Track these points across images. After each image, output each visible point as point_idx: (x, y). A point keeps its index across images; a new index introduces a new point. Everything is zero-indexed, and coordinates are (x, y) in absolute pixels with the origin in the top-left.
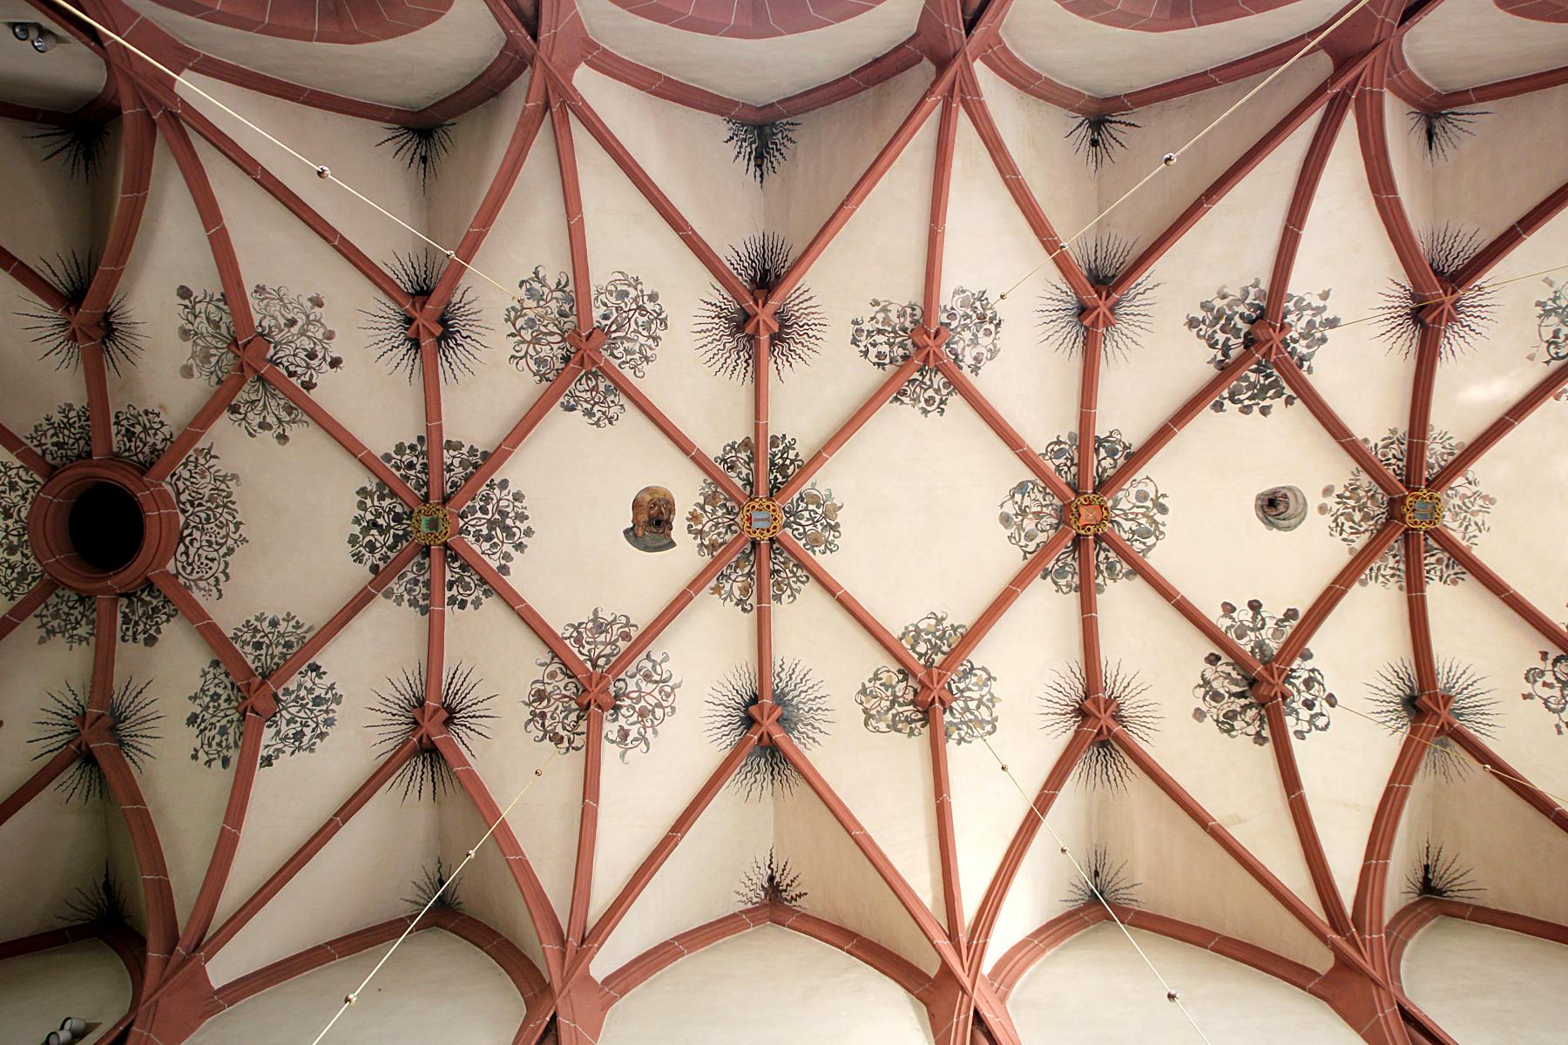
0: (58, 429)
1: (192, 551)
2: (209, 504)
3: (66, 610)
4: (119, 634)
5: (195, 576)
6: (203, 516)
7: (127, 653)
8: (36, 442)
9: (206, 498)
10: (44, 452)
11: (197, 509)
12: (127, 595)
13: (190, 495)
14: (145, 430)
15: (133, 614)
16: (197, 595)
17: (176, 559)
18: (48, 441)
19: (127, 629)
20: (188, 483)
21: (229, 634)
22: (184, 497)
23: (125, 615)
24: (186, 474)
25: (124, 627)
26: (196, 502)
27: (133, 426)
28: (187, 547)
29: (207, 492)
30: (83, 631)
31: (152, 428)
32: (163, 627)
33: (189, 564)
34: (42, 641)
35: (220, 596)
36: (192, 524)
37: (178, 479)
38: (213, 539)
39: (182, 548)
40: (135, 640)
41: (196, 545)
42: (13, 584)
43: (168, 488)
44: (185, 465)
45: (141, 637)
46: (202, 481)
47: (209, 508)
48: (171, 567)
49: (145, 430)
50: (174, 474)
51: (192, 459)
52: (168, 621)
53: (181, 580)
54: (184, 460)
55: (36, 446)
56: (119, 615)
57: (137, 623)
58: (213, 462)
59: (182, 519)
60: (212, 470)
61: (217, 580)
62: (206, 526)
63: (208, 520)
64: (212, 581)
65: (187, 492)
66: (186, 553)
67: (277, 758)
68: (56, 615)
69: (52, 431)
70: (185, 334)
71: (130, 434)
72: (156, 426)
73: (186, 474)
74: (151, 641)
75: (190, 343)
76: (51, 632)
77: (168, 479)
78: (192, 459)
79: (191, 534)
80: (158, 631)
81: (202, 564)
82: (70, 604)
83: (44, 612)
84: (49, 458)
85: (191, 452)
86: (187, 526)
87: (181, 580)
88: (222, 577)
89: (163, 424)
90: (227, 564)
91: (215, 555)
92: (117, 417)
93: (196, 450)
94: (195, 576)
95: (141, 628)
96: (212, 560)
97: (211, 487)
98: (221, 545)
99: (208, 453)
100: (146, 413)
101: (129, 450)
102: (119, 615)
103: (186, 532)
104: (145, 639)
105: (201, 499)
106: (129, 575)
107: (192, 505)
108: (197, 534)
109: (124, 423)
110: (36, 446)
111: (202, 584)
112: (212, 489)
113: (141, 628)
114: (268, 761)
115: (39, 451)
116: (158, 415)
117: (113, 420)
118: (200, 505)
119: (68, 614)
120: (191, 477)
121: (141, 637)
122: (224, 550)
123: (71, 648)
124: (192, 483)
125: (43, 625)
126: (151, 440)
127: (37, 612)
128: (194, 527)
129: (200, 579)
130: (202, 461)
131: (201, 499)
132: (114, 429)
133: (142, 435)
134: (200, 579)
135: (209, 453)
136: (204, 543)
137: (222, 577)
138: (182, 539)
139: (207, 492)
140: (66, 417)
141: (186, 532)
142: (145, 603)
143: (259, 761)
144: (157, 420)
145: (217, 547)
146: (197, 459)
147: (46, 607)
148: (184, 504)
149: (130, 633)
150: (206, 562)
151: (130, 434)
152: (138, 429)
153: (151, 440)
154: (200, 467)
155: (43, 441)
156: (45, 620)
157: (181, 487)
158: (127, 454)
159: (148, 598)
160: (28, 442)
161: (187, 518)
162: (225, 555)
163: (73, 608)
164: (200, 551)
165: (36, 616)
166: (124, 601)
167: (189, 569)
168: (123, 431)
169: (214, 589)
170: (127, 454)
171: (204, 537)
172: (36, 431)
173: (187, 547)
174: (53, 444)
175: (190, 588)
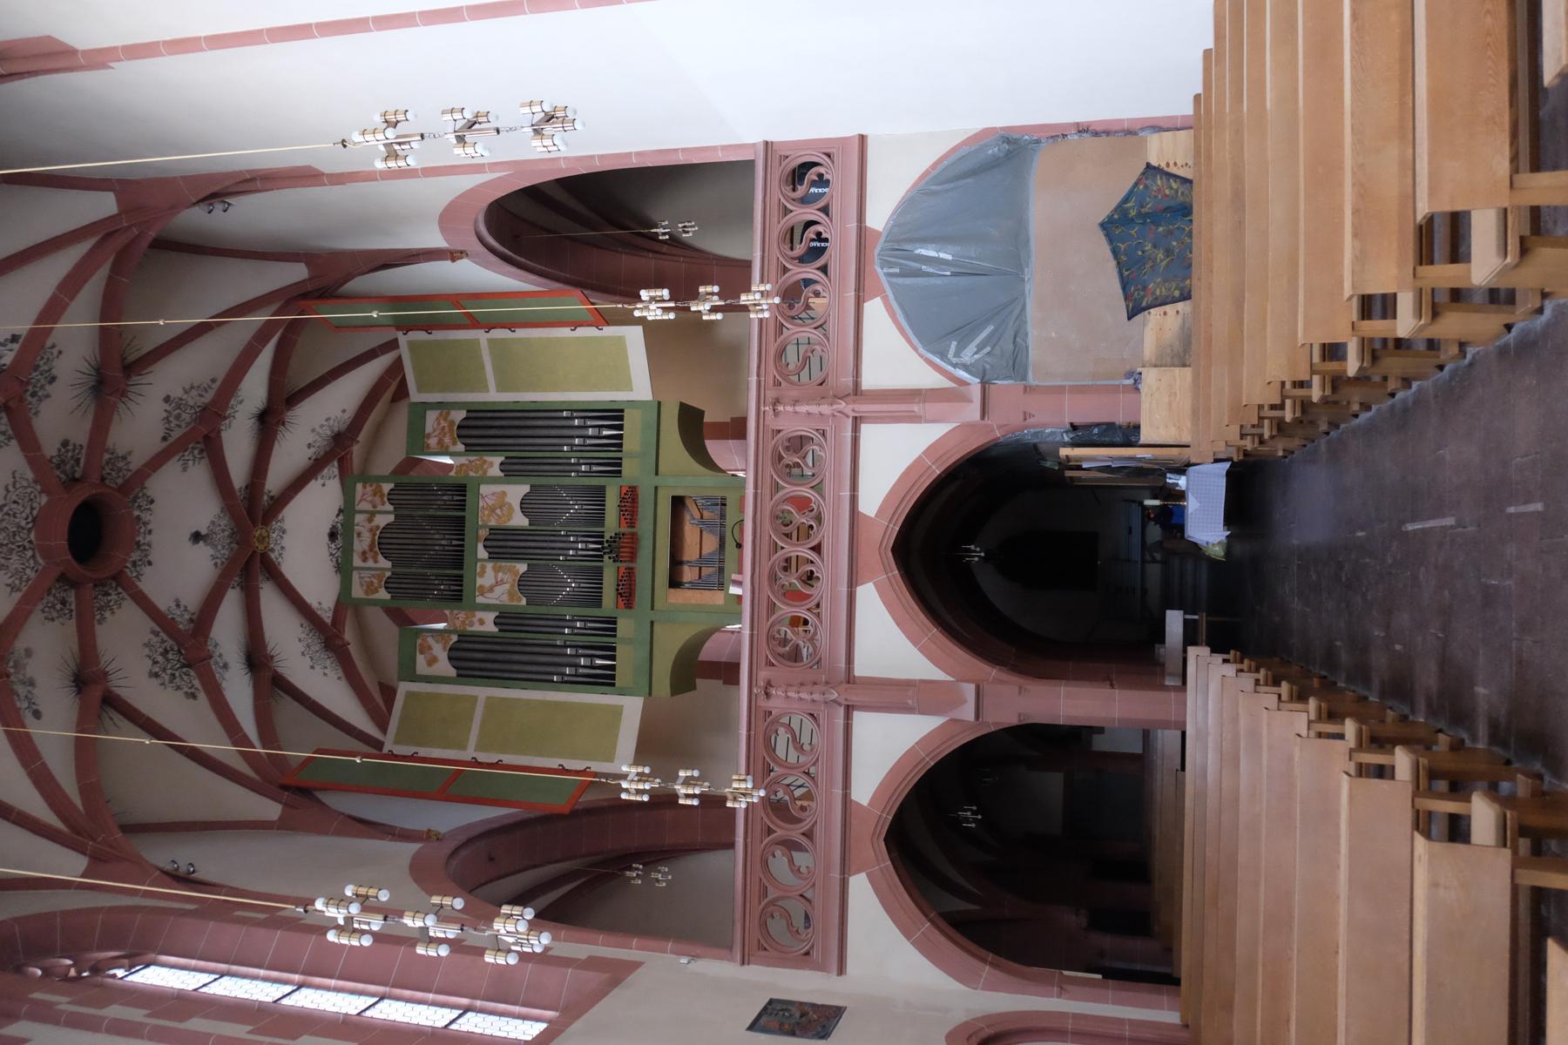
0: (107, 606)
1: (28, 510)
2: (13, 547)
3: (113, 473)
4: (84, 451)
5: (29, 490)
6: (18, 538)
7: (80, 434)
8: (121, 596)
9: (15, 551)
10: (116, 589)
11: (20, 544)
12: (76, 480)
13: (26, 555)
14: (53, 607)
15: (73, 467)
16: (30, 475)
17: (40, 504)
18: (114, 597)
19: (78, 454)
20: (27, 564)
21: (14, 442)
22: (29, 553)
23: (78, 464)
24: (28, 571)
25: (79, 456)
26: (21, 549)
27: (62, 610)
28: (31, 513)
29: (14, 557)
30: (107, 456)
31: (50, 607)
32: (55, 453)
33: (31, 500)
34: (130, 453)
35: (14, 473)
36: (25, 531)
37: (33, 567)
38: (12, 519)
39: (35, 512)
40: (75, 445)
41: (24, 515)
42: (140, 495)
43: (40, 561)
44: (28, 579)
45: (71, 447)
46: (17, 566)
47: (12, 543)
48: (44, 499)
49: (53, 607)
50: (37, 571)
51: (24, 584)
52: (52, 457)
53: (39, 488)
54: (30, 582)
55: (120, 593)
56: (82, 464)
57: (72, 457)
58: (10, 581)
59: (32, 536)
60: (10, 575)
61: (14, 487)
62: (14, 529)
63: (14, 535)
64: (18, 485)
65: (28, 557)
66: (32, 509)
67: (6, 340)
68: (120, 470)
69: (111, 604)
70: (32, 683)
71: (64, 603)
72: (47, 609)
73: (28, 571)
74: (65, 444)
75: (28, 676)
76: (124, 458)
77: (40, 568)
78: (24, 584)
79: (28, 523)
80: (59, 450)
81: (23, 500)
82: (110, 477)
83: (125, 472)
84: (114, 585)
85: (25, 589)
86: (29, 530)
87: (39, 488)
88: (11, 488)
89: (43, 611)
90: (5, 498)
91: (14, 506)
92: (71, 616)
93: (21, 591)
94: (29, 490)
95: (70, 454)
96: (15, 502)
97: (11, 561)
98: (7, 514)
99: (13, 588)
100: (53, 620)
101: (65, 590)
102: (82, 464)
103: (30, 525)
104: (68, 445)
105: (18, 552)
106: (81, 494)
107: (24, 547)
108: (23, 523)
109: (67, 611)
110: (120, 593)
111: (25, 484)
112: (10, 559)
113: (70, 454)
114: (14, 339)
115: (120, 590)
116: (46, 618)
117: (74, 613)
118: (19, 547)
119: (112, 470)
120: (24, 569)
121: (71, 447)
122: (6, 509)
123: (114, 445)
124: (23, 564)
125: (128, 463)
126: (51, 598)
127: (130, 474)
128: (23, 529)
129: (26, 488)
130: (17, 582)
131: (18, 552)
132: (73, 607)
133: (56, 602)
134: (26, 488)
135: (12, 588)
136: (18, 515)
137: (11, 488)
138: (34, 520)
139: (14, 557)
140: (102, 615)
141: (30, 525)
142: (64, 472)
143: (21, 340)
144: (46, 614)
145: (11, 512)
146: (21, 584)
147: (124, 476)
148: (30, 548)
149: (77, 451)
150: (20, 501)
151: (64, 603)
152: (59, 606)
153: (51, 598)
154: (18, 577)
155: (116, 597)
156: (125, 467)
157: (31, 562)
158: (66, 587)
159: (62, 476)
160: (126, 596)
161: (29, 537)
162: (4, 505)
163: (109, 474)
164: (22, 509)
165: (130, 470)
166: (77, 475)
167: (32, 497)
168: (67, 605)
169: (17, 479)
170: (66, 587)
171: (17, 520)
172: (120, 604)
173: (31, 513)
174: (110, 595)
175: (35, 482)
